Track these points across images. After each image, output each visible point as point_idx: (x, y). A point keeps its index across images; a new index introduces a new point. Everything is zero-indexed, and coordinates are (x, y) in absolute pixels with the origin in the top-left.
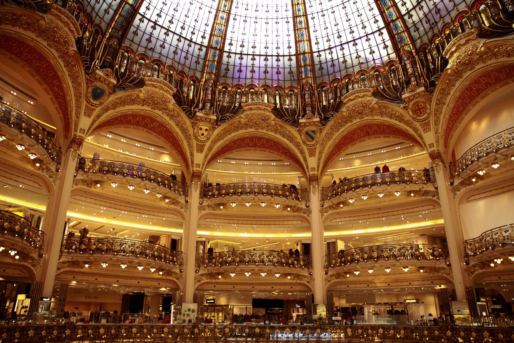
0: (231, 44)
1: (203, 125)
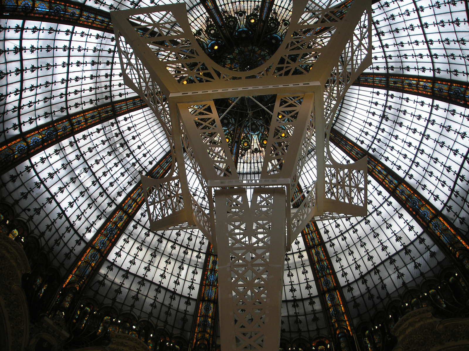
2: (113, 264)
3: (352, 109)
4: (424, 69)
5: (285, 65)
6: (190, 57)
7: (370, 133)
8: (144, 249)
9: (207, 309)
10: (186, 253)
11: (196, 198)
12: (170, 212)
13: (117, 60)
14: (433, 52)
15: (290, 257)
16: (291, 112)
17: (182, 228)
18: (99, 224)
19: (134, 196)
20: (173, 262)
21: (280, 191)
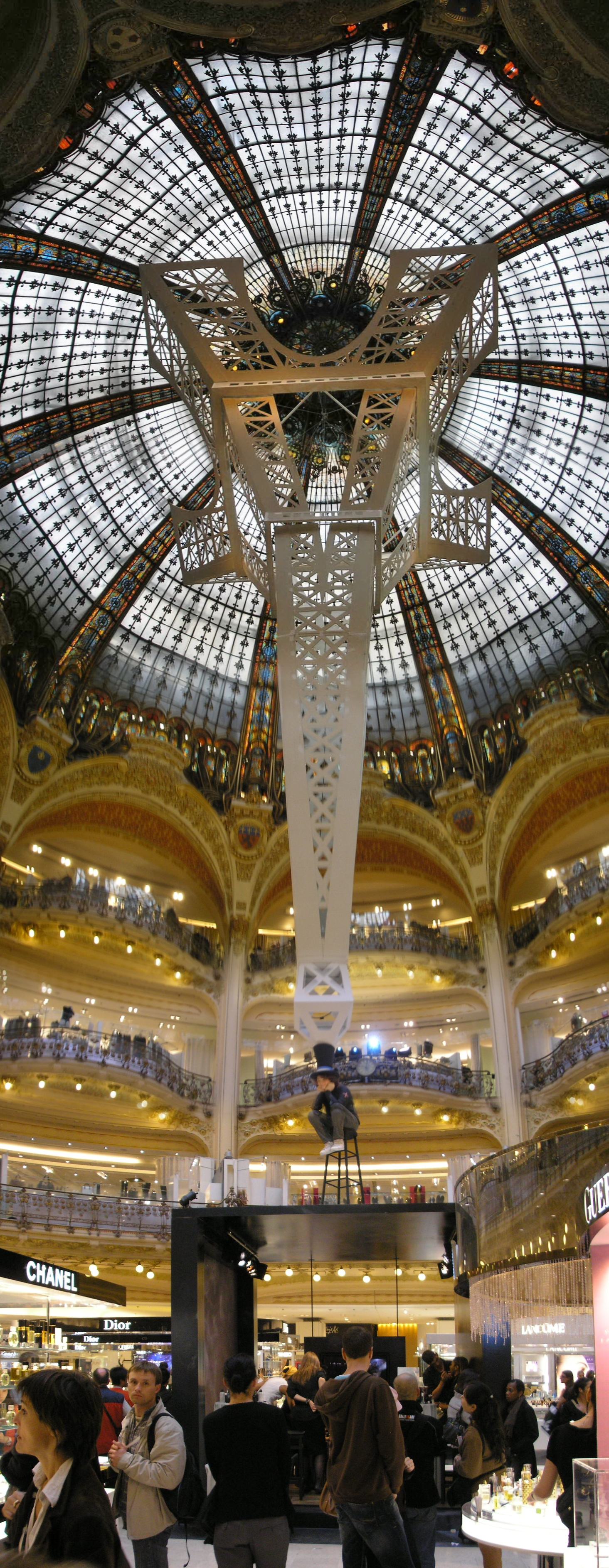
2: (129, 632)
3: (470, 410)
5: (377, 348)
6: (244, 333)
8: (174, 610)
9: (263, 698)
10: (232, 616)
11: (248, 538)
12: (211, 558)
13: (142, 332)
15: (380, 621)
16: (382, 415)
17: (227, 581)
18: (111, 574)
19: (161, 534)
20: (213, 628)
21: (368, 529)
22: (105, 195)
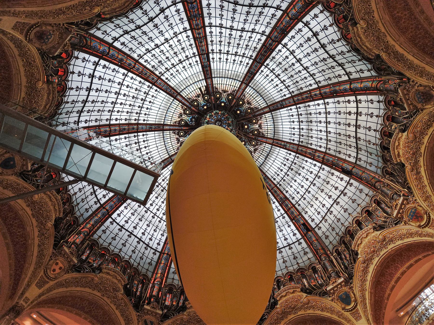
0: (119, 215)
1: (61, 262)
4: (311, 85)
7: (296, 133)
14: (311, 73)
22: (93, 102)
